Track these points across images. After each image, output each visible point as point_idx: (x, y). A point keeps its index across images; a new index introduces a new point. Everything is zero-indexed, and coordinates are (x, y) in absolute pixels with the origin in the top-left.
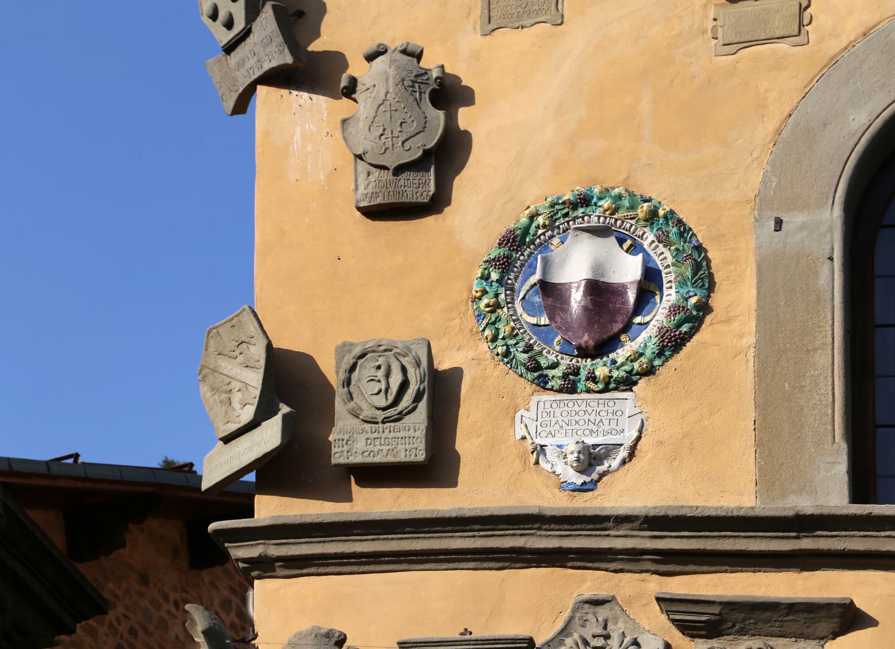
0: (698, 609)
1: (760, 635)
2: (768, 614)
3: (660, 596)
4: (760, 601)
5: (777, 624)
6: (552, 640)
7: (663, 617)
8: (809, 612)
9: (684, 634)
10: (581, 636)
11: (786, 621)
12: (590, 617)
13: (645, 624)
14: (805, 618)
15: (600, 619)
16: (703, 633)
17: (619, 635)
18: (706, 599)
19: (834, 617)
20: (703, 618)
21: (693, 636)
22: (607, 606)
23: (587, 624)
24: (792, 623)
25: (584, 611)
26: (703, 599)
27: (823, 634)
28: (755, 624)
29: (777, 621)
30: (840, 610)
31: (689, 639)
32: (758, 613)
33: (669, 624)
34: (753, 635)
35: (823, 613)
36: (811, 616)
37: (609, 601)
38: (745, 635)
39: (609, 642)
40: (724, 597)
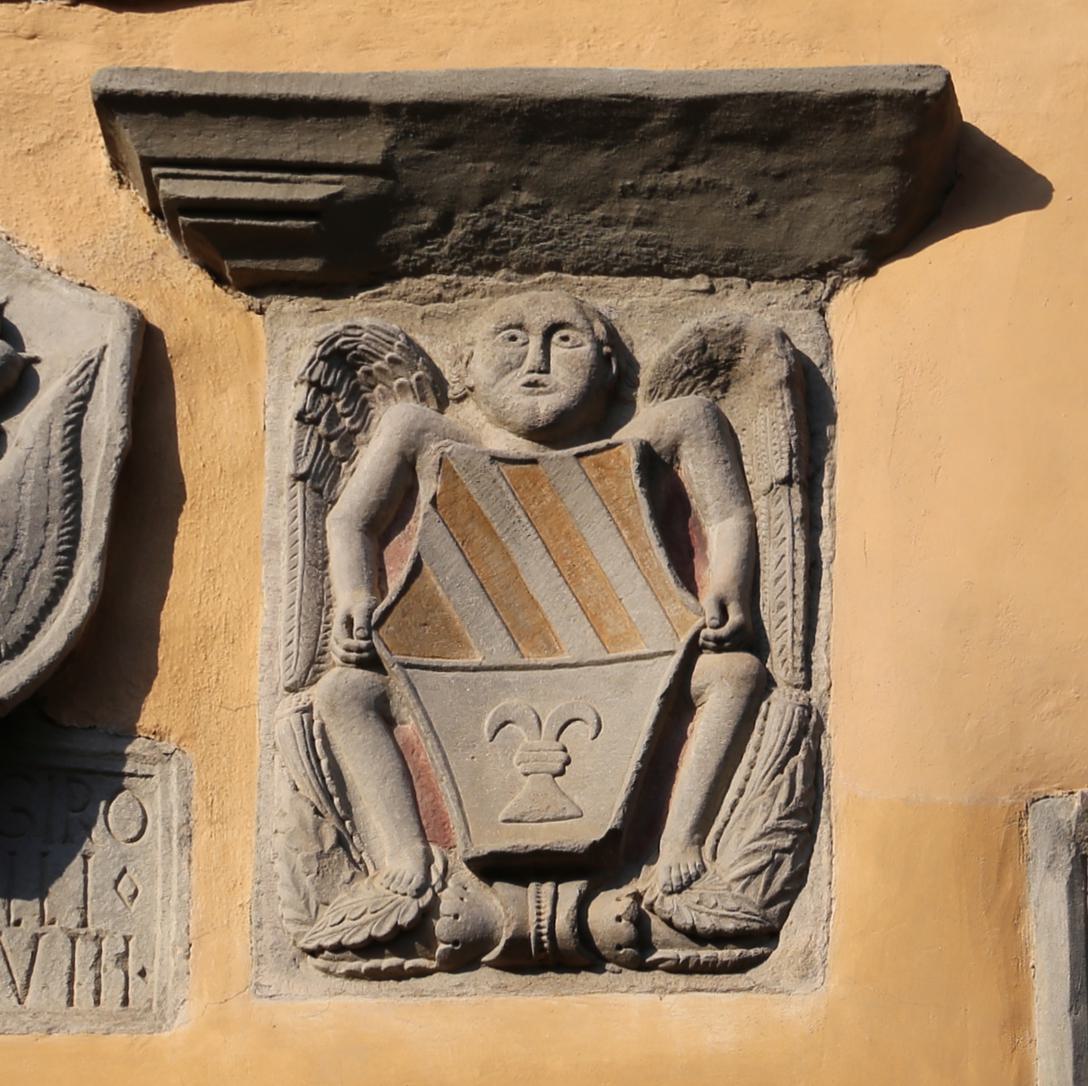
0: (288, 144)
1: (556, 266)
2: (595, 159)
4: (567, 91)
5: (634, 208)
7: (129, 204)
8: (773, 141)
9: (219, 279)
11: (670, 193)
14: (753, 176)
16: (308, 265)
18: (328, 92)
19: (871, 164)
20: (312, 191)
21: (259, 286)
24: (695, 202)
26: (311, 91)
27: (822, 252)
28: (539, 210)
29: (625, 193)
30: (899, 127)
31: (239, 302)
32: (553, 154)
33: (154, 236)
34: (529, 268)
35: (832, 144)
36: (778, 161)
38: (492, 268)
40: (408, 79)
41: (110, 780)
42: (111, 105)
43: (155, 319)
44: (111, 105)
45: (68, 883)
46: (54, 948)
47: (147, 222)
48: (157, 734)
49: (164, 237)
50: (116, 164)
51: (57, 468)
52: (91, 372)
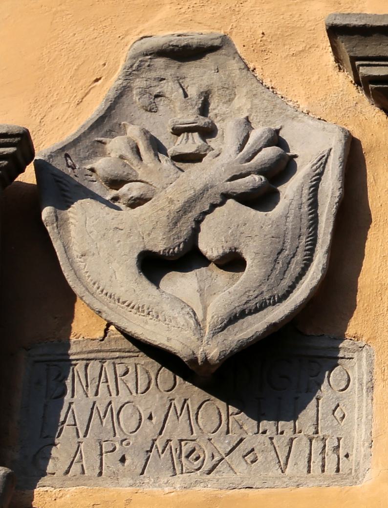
3: (339, 21)
6: (75, 143)
7: (344, 79)
10: (146, 132)
12: (169, 87)
13: (298, 95)
15: (193, 92)
17: (239, 123)
22: (209, 60)
23: (161, 103)
25: (154, 75)
33: (357, 95)
37: (213, 49)
39: (212, 142)
41: (332, 361)
42: (335, 32)
43: (356, 135)
44: (335, 32)
45: (310, 411)
46: (301, 446)
47: (353, 88)
48: (356, 337)
49: (362, 95)
50: (338, 60)
51: (305, 209)
52: (323, 161)
